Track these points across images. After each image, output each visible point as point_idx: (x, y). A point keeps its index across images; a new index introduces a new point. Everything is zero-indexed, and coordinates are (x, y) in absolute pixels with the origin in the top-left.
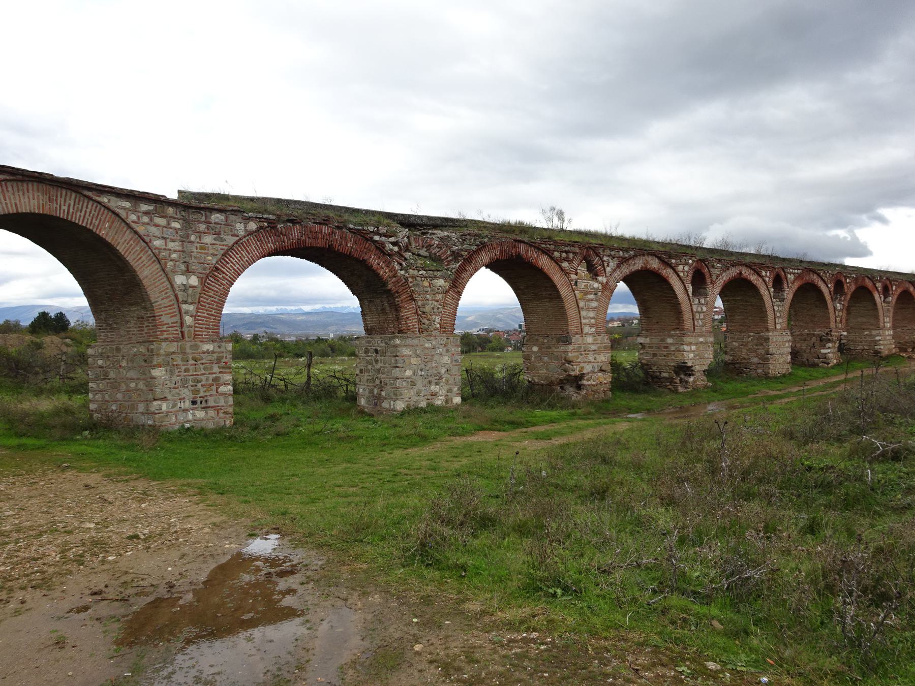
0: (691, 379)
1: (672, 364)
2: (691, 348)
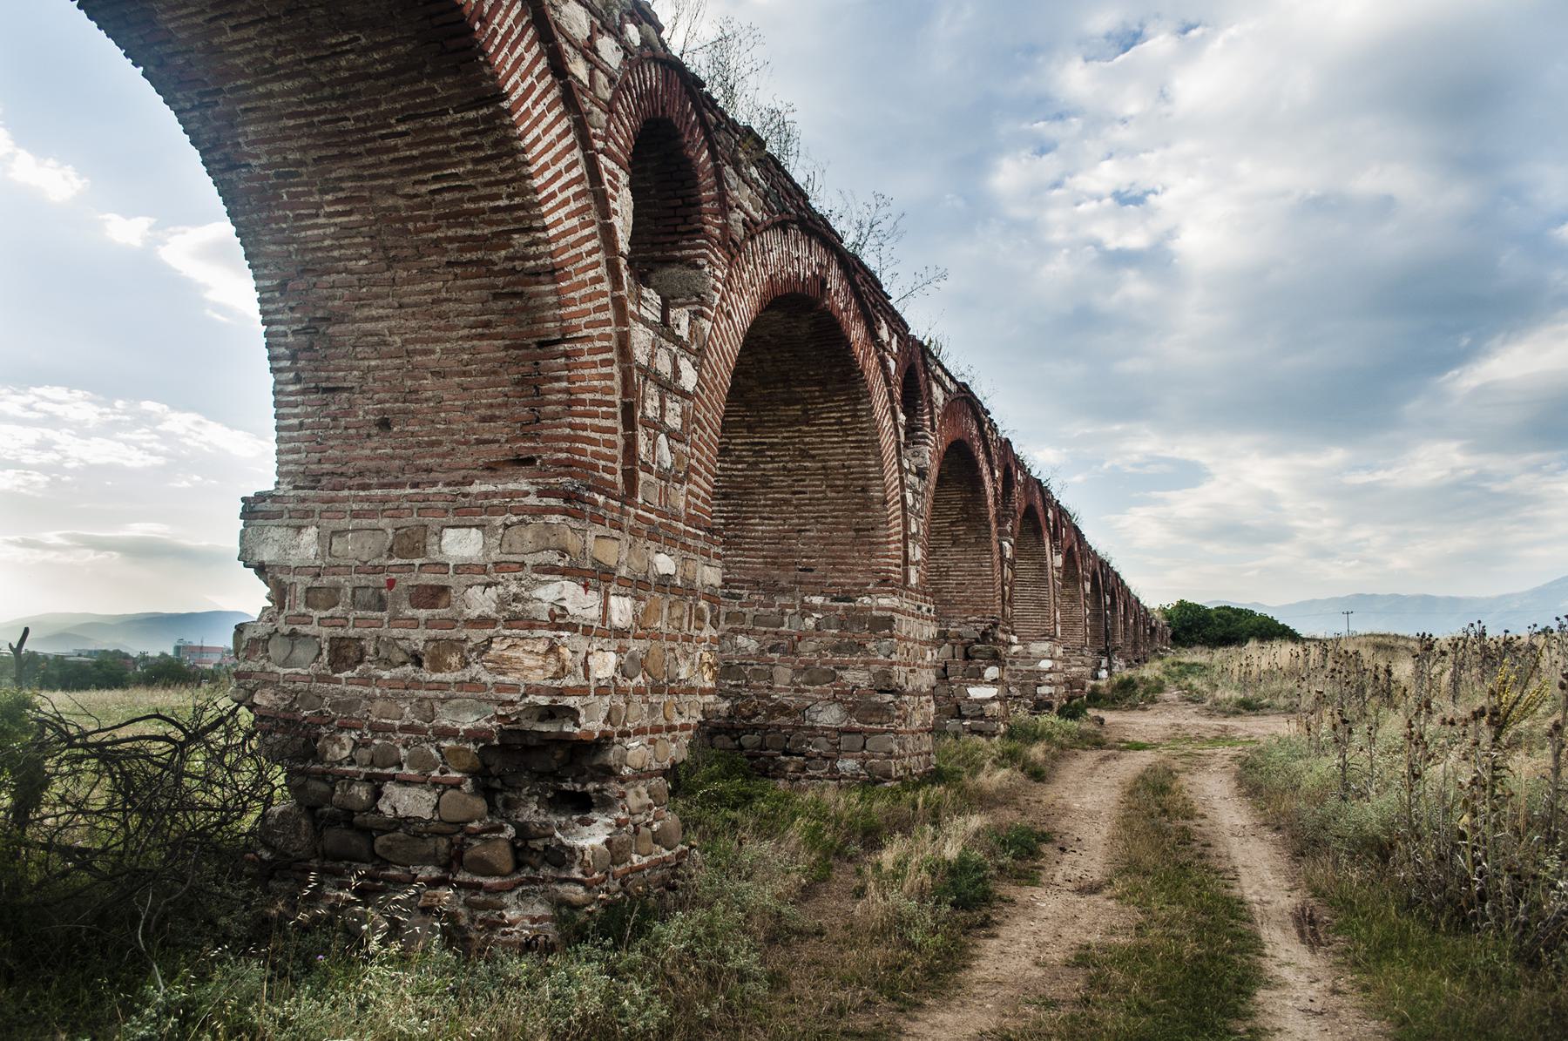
0: (592, 837)
1: (468, 722)
2: (605, 608)
